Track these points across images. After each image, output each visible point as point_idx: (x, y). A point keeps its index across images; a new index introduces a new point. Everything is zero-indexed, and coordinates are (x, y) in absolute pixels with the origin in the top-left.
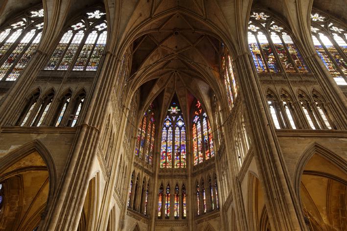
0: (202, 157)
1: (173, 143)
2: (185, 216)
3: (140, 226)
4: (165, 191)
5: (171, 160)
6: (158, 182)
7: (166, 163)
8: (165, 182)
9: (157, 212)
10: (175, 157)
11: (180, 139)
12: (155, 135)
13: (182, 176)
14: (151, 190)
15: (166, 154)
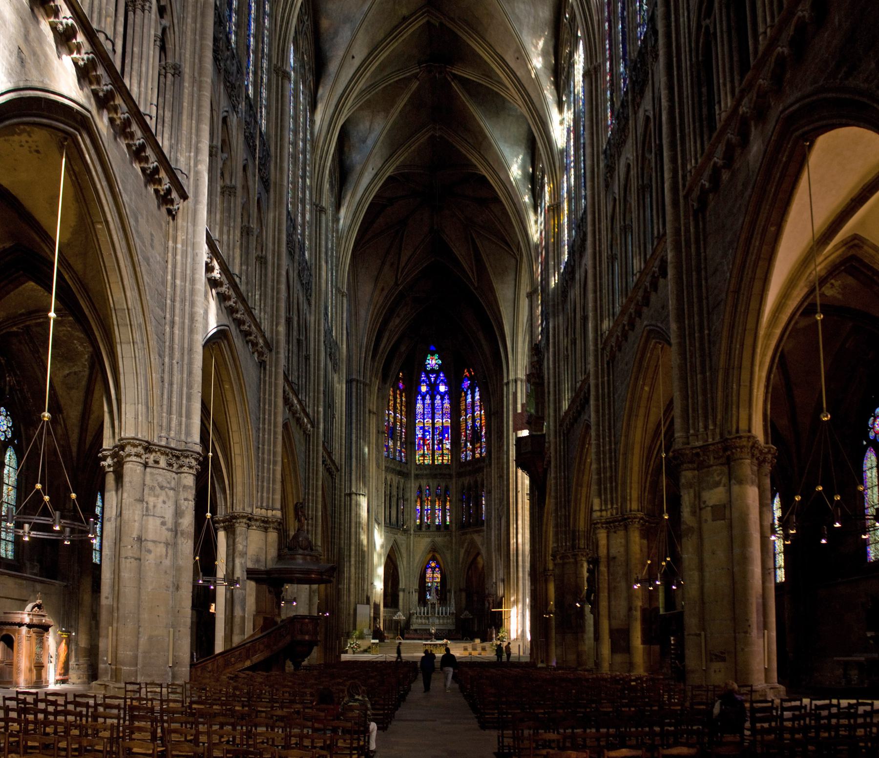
0: (471, 451)
1: (433, 423)
2: (448, 523)
3: (399, 541)
4: (424, 496)
5: (430, 452)
6: (415, 484)
7: (423, 455)
8: (424, 483)
9: (415, 521)
10: (436, 447)
11: (442, 417)
12: (406, 412)
13: (445, 475)
14: (408, 495)
15: (423, 442)
